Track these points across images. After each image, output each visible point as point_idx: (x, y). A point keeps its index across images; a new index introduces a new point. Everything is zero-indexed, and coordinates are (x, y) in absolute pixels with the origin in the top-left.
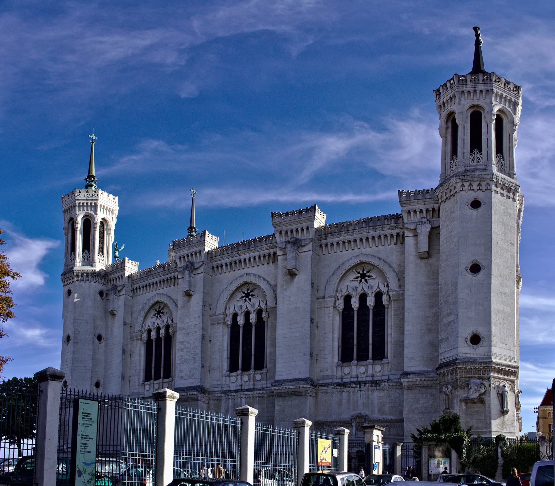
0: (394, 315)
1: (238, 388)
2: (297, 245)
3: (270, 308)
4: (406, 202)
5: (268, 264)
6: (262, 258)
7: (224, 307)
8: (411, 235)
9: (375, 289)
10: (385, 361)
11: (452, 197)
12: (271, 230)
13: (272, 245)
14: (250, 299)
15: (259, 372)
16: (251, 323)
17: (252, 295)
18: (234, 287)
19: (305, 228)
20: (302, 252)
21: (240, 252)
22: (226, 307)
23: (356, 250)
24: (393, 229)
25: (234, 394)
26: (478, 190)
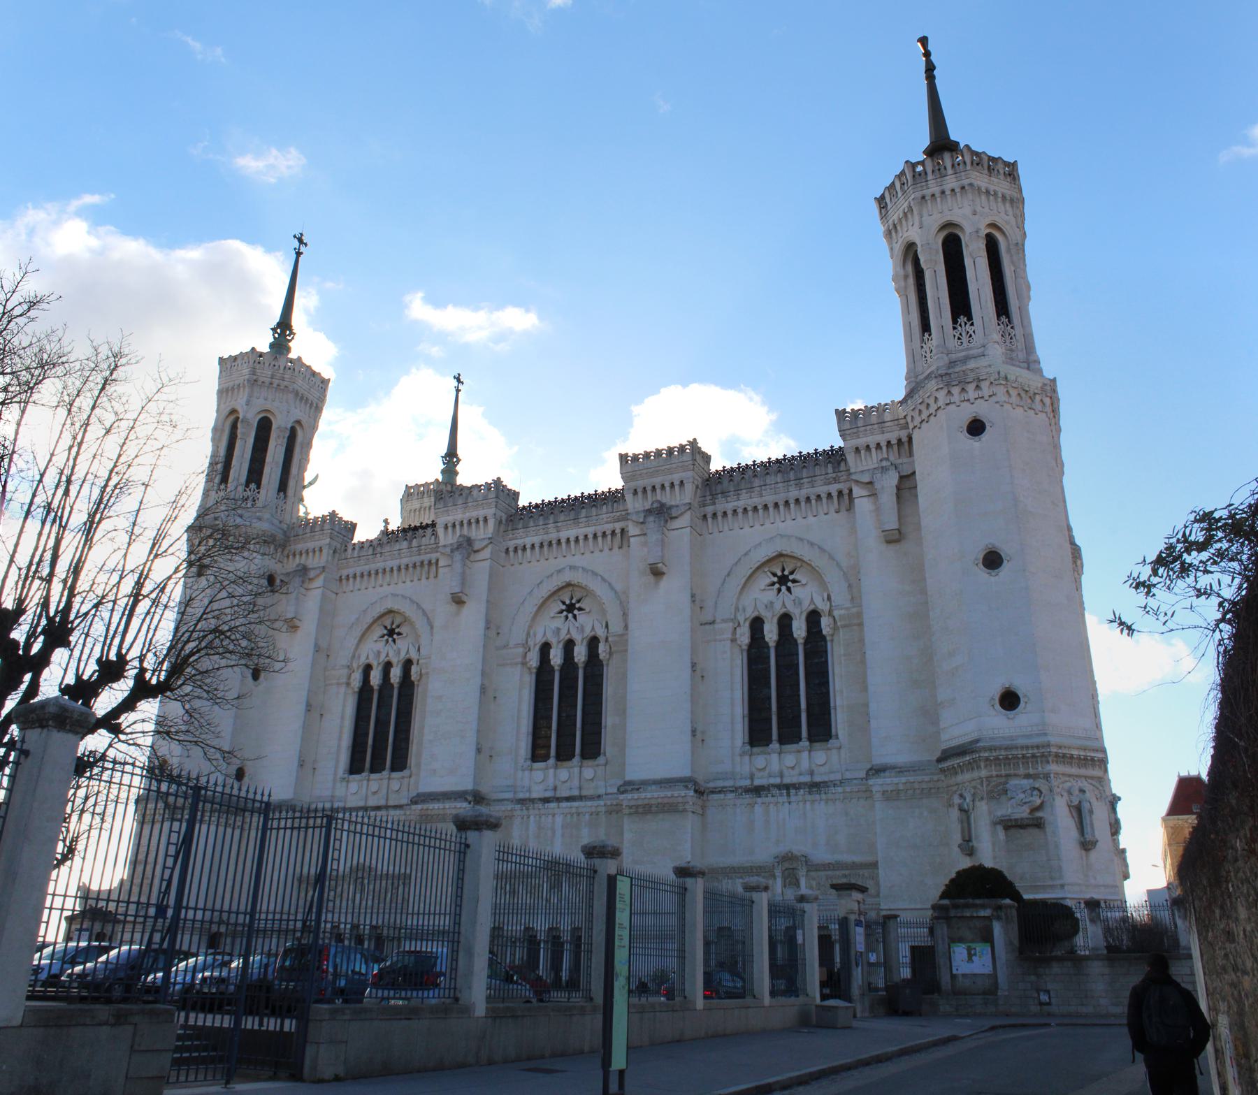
0: (845, 655)
1: (549, 794)
4: (850, 431)
5: (611, 549)
6: (600, 539)
7: (525, 632)
8: (865, 493)
14: (575, 617)
19: (677, 483)
21: (559, 524)
22: (528, 634)
24: (830, 483)
25: (540, 806)
26: (976, 399)
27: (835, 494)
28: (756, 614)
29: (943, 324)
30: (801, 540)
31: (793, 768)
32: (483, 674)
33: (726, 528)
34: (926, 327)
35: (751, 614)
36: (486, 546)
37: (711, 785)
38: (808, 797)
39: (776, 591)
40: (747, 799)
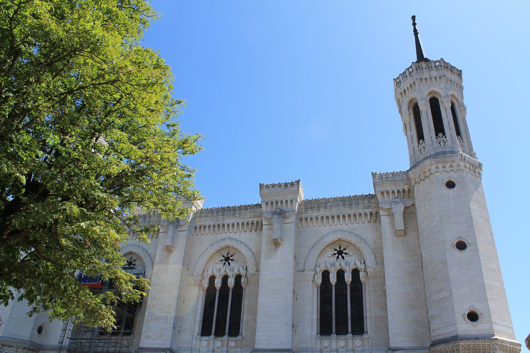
2: (283, 216)
3: (251, 274)
5: (250, 231)
6: (245, 226)
7: (203, 269)
11: (427, 178)
12: (258, 200)
13: (256, 214)
14: (229, 264)
15: (234, 339)
17: (232, 260)
18: (215, 249)
20: (286, 223)
21: (224, 216)
22: (204, 271)
27: (369, 214)
28: (325, 268)
30: (351, 233)
31: (343, 348)
33: (312, 226)
34: (420, 136)
35: (323, 268)
39: (336, 258)
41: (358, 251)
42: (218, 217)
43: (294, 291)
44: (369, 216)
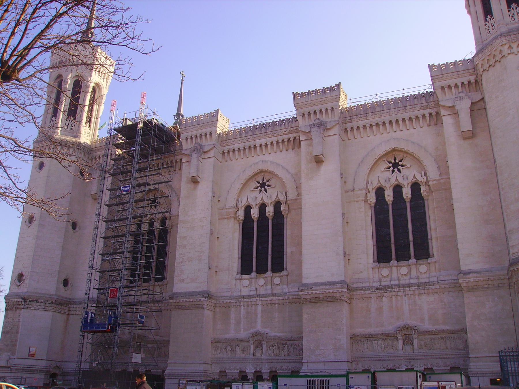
1: (252, 293)
3: (291, 200)
5: (287, 150)
6: (280, 144)
9: (411, 179)
10: (430, 260)
13: (292, 129)
14: (266, 190)
15: (278, 274)
16: (267, 217)
17: (269, 186)
19: (329, 109)
20: (328, 136)
21: (255, 136)
22: (237, 201)
23: (385, 135)
27: (427, 115)
29: (502, 8)
31: (406, 275)
32: (211, 223)
33: (359, 136)
35: (375, 185)
36: (212, 149)
37: (355, 286)
38: (417, 292)
39: (391, 172)
40: (378, 293)
41: (418, 161)
42: (248, 137)
43: (343, 214)
44: (428, 118)
